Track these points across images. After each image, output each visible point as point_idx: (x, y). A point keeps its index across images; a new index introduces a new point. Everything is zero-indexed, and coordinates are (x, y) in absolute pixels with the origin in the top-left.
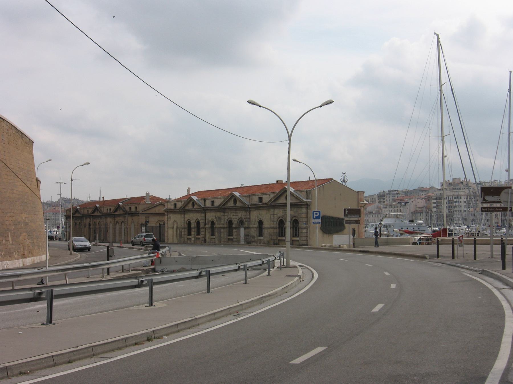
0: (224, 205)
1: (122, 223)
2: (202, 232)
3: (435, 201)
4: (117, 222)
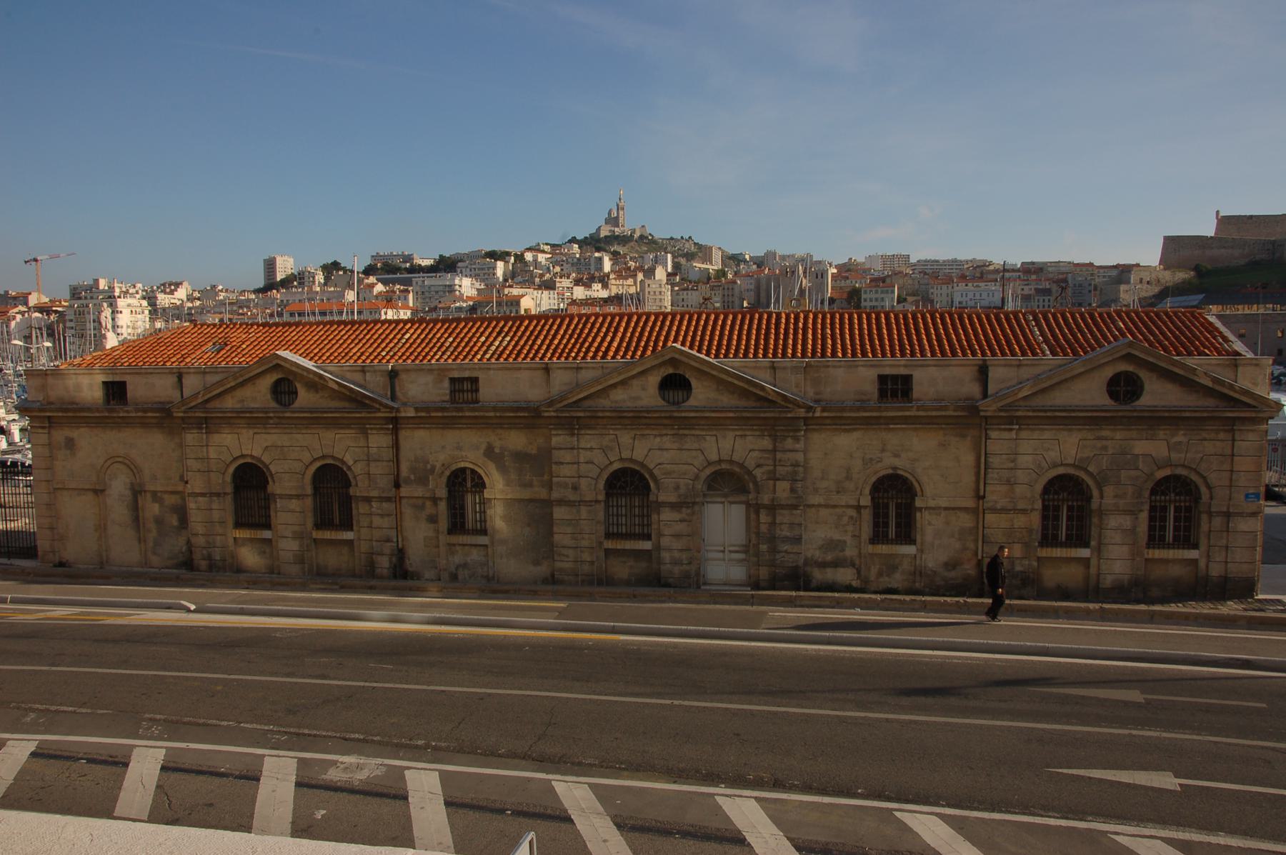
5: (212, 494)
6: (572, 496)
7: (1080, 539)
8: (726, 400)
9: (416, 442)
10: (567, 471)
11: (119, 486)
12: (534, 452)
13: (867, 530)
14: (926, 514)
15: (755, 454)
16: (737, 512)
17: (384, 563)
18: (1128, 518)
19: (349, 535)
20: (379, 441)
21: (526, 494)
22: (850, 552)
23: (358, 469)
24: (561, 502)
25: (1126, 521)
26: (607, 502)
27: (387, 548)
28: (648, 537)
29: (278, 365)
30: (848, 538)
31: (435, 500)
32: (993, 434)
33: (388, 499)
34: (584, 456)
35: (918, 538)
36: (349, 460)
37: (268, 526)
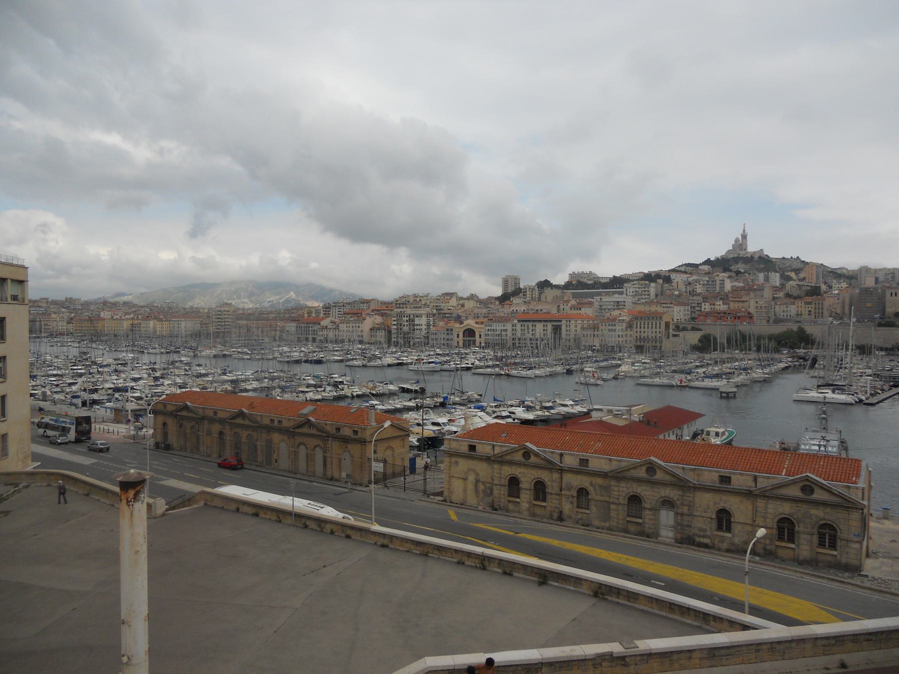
0: (619, 472)
1: (315, 447)
3: (395, 319)
4: (300, 444)
5: (501, 485)
6: (616, 501)
7: (791, 539)
8: (668, 478)
9: (568, 478)
10: (615, 493)
11: (471, 478)
12: (605, 485)
14: (736, 524)
15: (677, 496)
16: (671, 514)
17: (556, 515)
19: (544, 504)
20: (556, 476)
21: (602, 498)
22: (708, 533)
23: (549, 483)
24: (613, 503)
25: (809, 537)
26: (628, 505)
27: (557, 510)
28: (641, 518)
29: (525, 448)
30: (708, 528)
31: (573, 497)
32: (758, 500)
33: (558, 495)
34: (621, 489)
35: (732, 531)
36: (546, 480)
37: (519, 497)
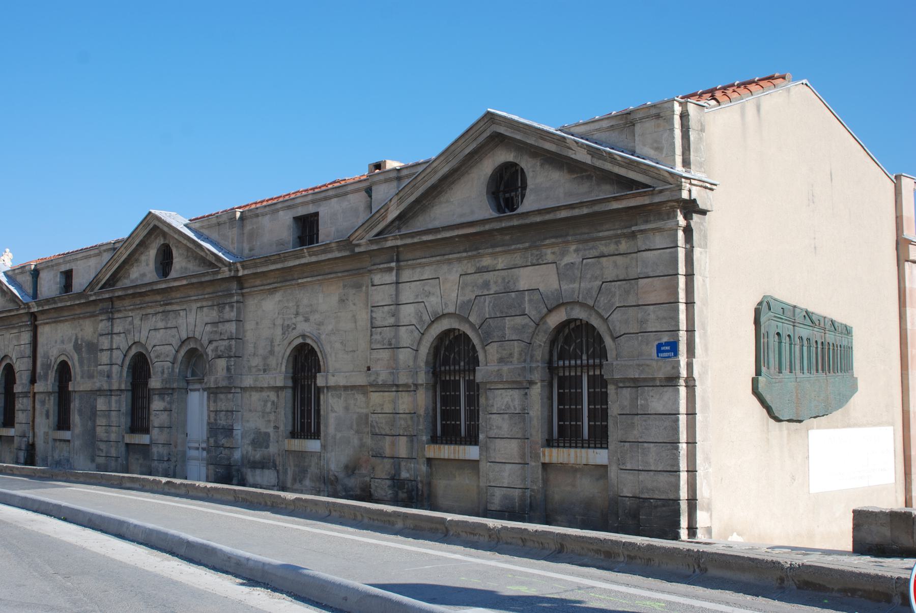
0: (113, 280)
2: (20, 413)
13: (284, 419)
18: (516, 394)
30: (270, 430)
